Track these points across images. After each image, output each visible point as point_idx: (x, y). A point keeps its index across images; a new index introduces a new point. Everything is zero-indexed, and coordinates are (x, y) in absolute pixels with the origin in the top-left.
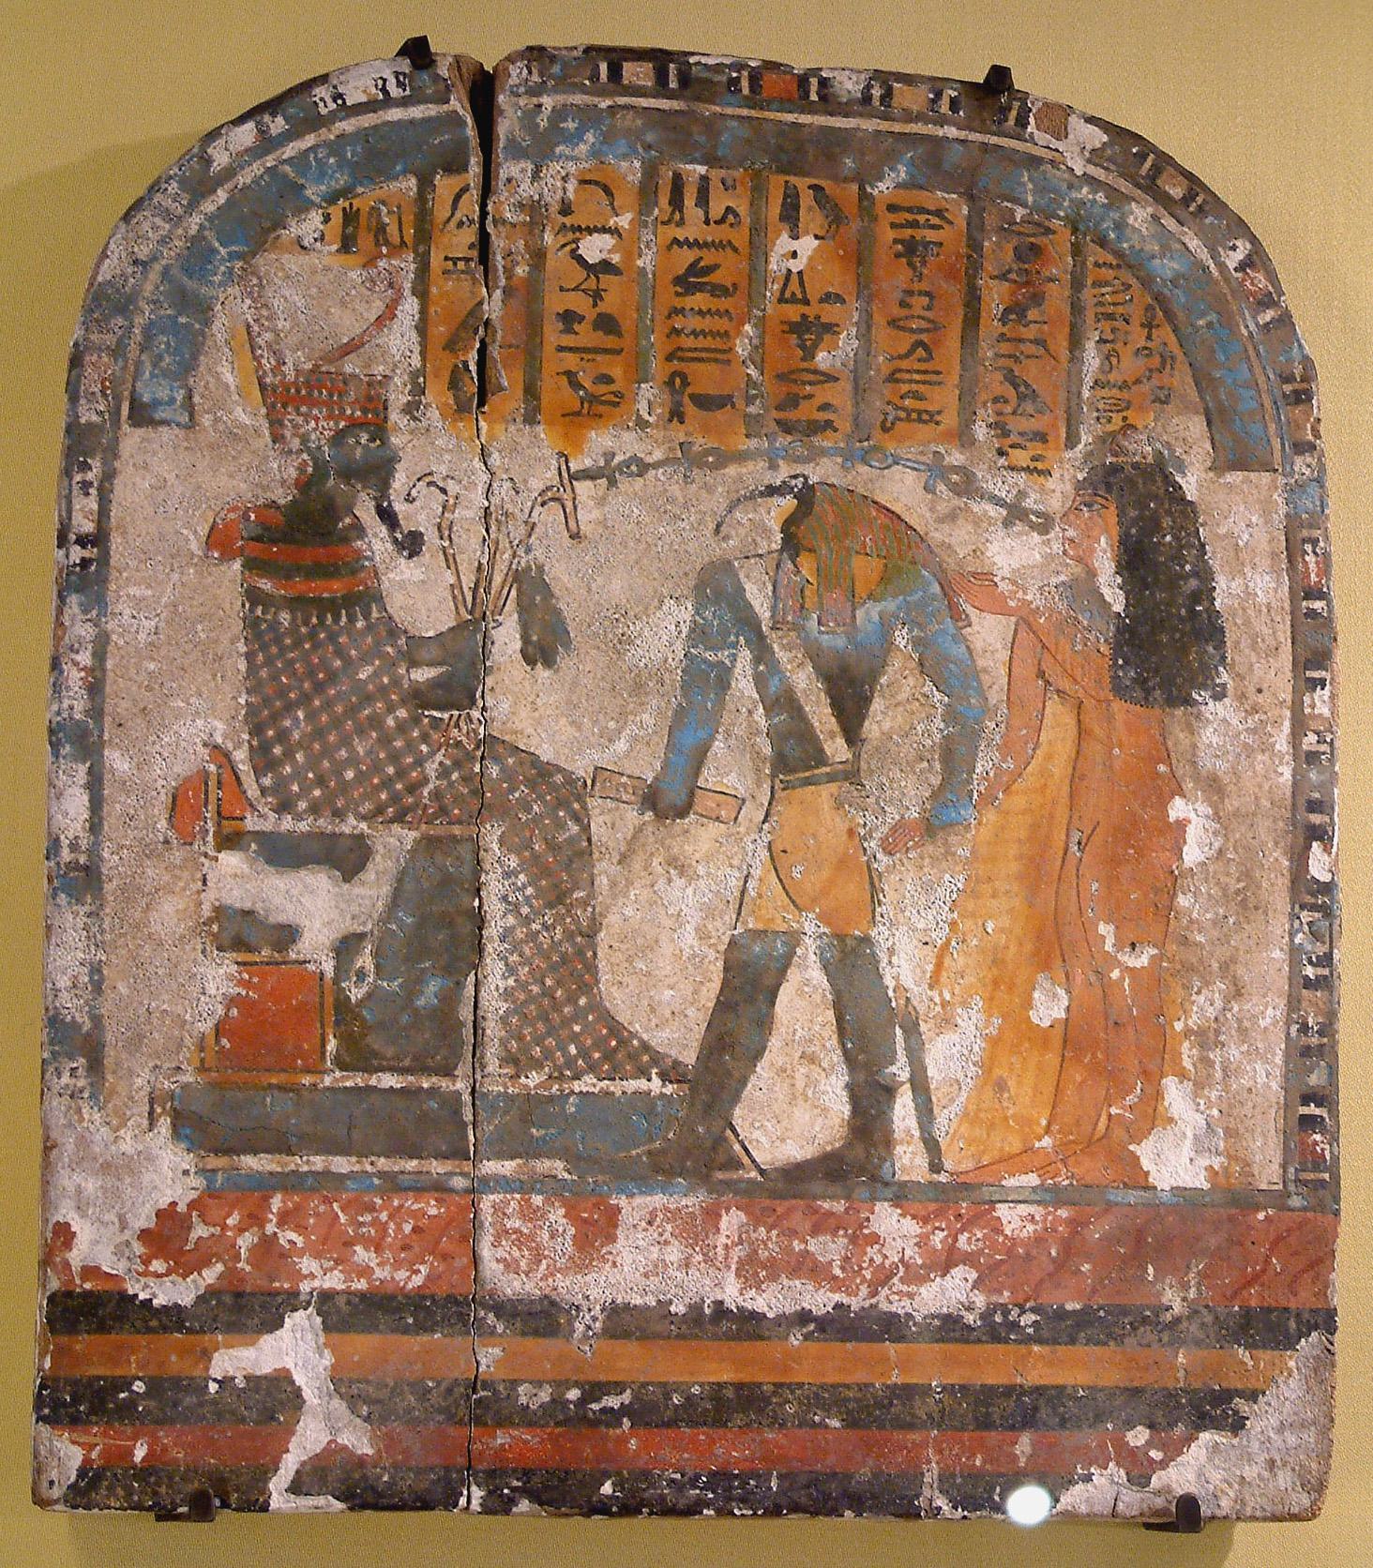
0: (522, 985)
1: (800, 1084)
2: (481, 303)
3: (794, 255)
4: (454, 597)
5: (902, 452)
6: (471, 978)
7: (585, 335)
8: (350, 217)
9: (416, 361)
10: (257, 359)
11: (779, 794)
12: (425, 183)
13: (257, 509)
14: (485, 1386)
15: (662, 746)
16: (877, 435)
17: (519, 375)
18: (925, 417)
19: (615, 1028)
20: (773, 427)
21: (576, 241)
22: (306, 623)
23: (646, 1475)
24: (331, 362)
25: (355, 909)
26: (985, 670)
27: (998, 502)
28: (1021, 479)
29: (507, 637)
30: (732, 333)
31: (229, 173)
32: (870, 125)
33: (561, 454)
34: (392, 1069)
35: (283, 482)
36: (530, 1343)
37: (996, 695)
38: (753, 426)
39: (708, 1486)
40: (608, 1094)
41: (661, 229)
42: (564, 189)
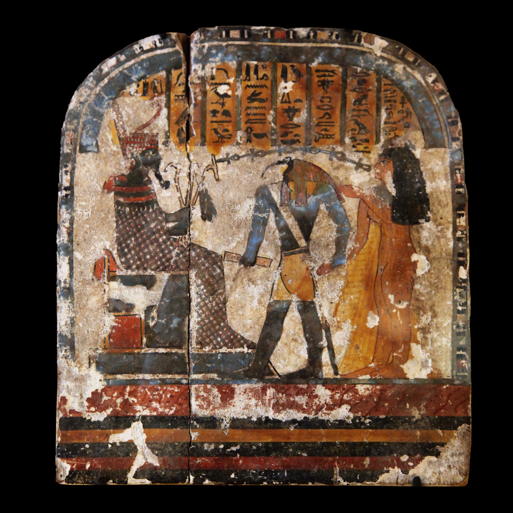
0: (203, 320)
1: (292, 348)
2: (187, 109)
3: (286, 88)
4: (180, 201)
5: (321, 148)
6: (187, 318)
7: (219, 117)
8: (145, 85)
9: (167, 128)
10: (117, 130)
11: (284, 258)
12: (169, 73)
13: (118, 176)
14: (194, 444)
15: (246, 244)
16: (314, 144)
17: (199, 131)
18: (329, 136)
19: (233, 333)
20: (280, 142)
21: (216, 88)
22: (134, 211)
23: (245, 471)
24: (140, 130)
25: (150, 298)
26: (350, 216)
27: (354, 162)
28: (361, 155)
29: (196, 212)
30: (266, 114)
31: (108, 74)
32: (310, 45)
33: (212, 155)
34: (163, 347)
35: (126, 168)
36: (208, 431)
37: (353, 224)
38: (274, 143)
39: (265, 475)
40: (231, 353)
41: (243, 82)
42: (212, 72)
